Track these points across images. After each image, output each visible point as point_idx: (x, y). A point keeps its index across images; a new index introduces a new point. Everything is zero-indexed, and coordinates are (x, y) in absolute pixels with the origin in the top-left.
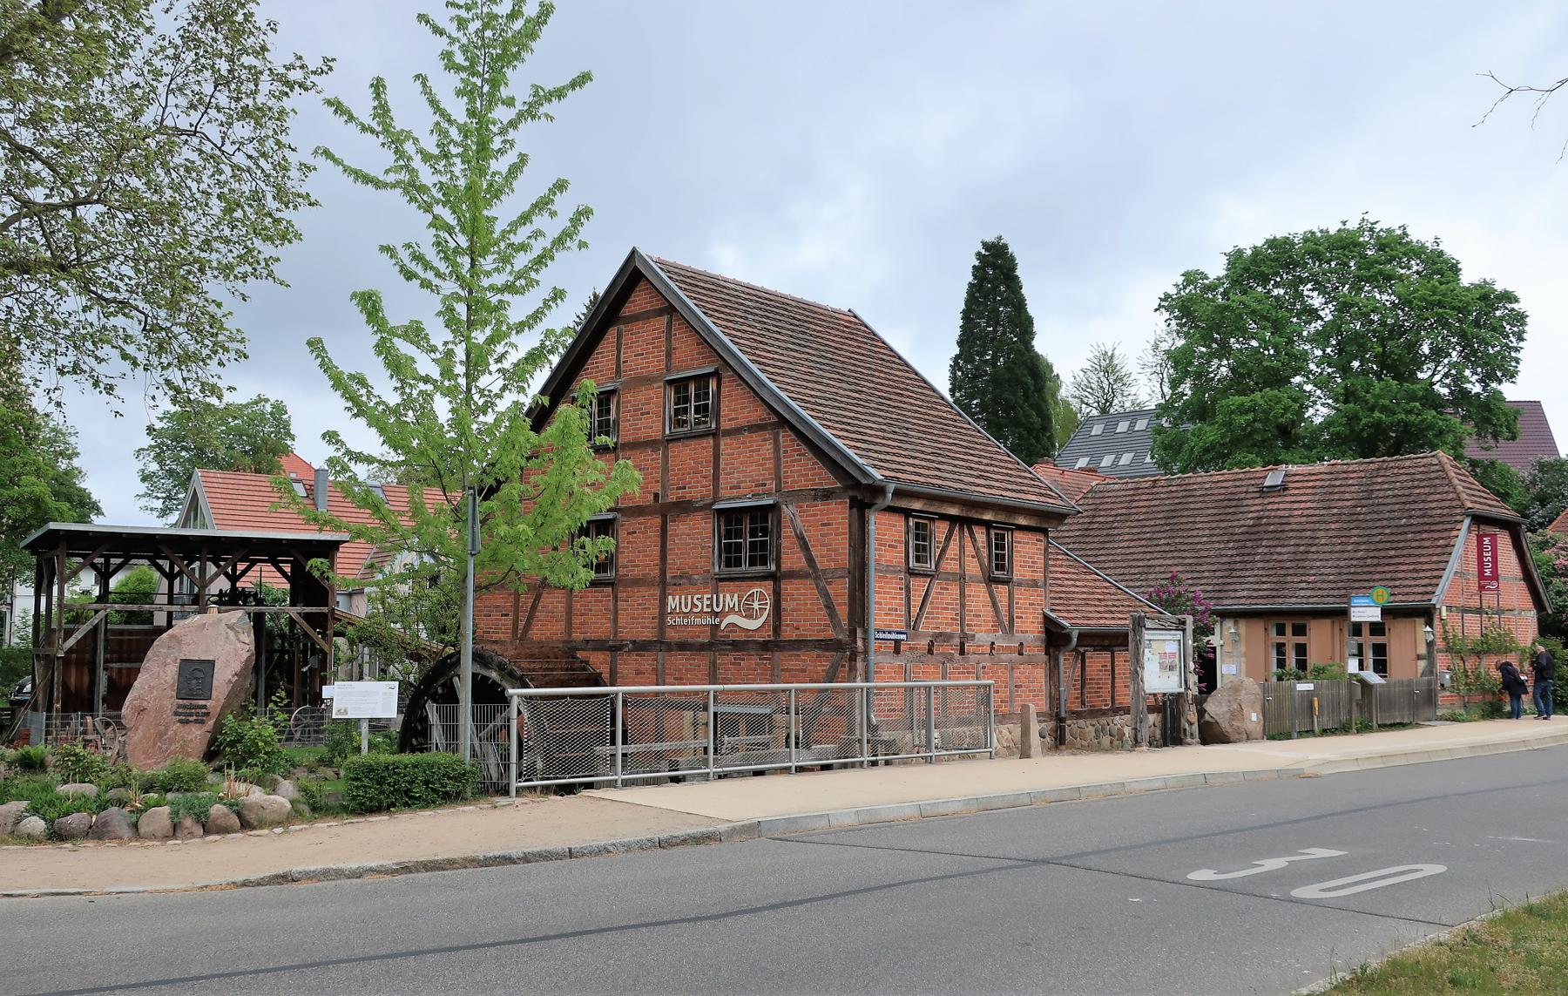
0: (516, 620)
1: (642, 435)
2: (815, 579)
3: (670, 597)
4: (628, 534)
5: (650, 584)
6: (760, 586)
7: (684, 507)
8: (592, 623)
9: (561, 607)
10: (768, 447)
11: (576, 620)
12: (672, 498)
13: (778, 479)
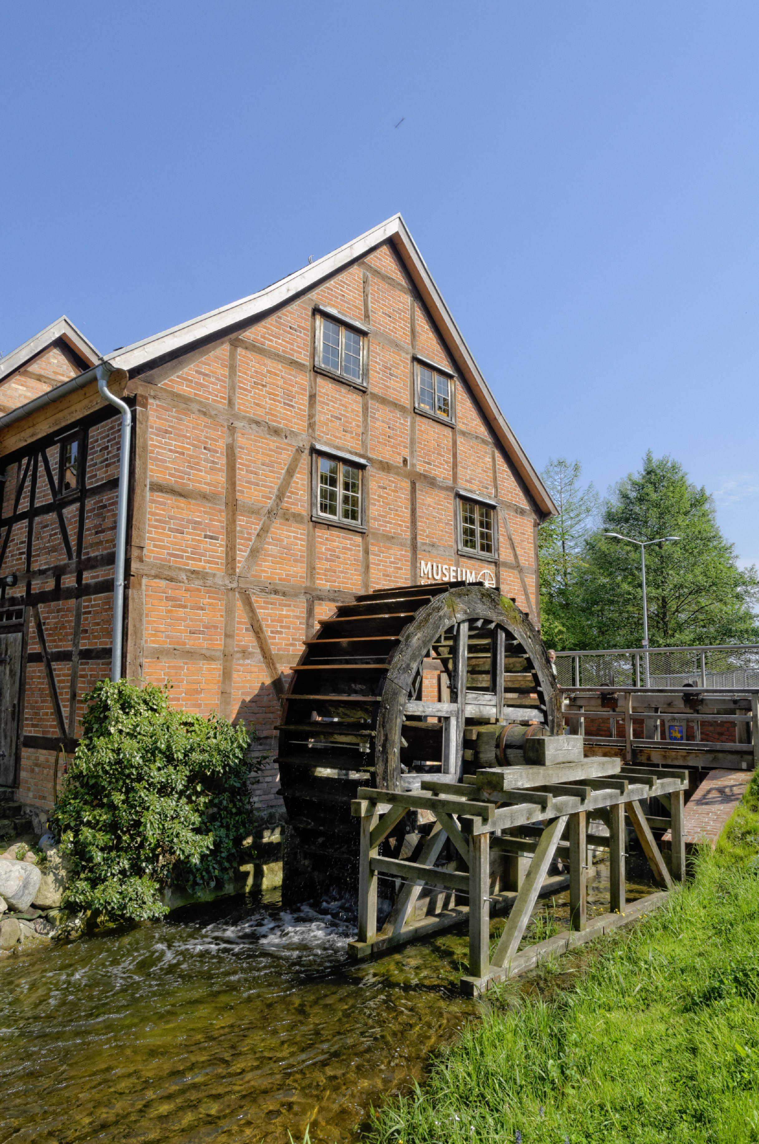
1: (392, 396)
2: (520, 572)
3: (423, 562)
4: (379, 487)
5: (402, 545)
6: (488, 568)
7: (431, 482)
8: (342, 572)
9: (300, 547)
10: (488, 459)
11: (321, 566)
12: (420, 468)
13: (496, 487)
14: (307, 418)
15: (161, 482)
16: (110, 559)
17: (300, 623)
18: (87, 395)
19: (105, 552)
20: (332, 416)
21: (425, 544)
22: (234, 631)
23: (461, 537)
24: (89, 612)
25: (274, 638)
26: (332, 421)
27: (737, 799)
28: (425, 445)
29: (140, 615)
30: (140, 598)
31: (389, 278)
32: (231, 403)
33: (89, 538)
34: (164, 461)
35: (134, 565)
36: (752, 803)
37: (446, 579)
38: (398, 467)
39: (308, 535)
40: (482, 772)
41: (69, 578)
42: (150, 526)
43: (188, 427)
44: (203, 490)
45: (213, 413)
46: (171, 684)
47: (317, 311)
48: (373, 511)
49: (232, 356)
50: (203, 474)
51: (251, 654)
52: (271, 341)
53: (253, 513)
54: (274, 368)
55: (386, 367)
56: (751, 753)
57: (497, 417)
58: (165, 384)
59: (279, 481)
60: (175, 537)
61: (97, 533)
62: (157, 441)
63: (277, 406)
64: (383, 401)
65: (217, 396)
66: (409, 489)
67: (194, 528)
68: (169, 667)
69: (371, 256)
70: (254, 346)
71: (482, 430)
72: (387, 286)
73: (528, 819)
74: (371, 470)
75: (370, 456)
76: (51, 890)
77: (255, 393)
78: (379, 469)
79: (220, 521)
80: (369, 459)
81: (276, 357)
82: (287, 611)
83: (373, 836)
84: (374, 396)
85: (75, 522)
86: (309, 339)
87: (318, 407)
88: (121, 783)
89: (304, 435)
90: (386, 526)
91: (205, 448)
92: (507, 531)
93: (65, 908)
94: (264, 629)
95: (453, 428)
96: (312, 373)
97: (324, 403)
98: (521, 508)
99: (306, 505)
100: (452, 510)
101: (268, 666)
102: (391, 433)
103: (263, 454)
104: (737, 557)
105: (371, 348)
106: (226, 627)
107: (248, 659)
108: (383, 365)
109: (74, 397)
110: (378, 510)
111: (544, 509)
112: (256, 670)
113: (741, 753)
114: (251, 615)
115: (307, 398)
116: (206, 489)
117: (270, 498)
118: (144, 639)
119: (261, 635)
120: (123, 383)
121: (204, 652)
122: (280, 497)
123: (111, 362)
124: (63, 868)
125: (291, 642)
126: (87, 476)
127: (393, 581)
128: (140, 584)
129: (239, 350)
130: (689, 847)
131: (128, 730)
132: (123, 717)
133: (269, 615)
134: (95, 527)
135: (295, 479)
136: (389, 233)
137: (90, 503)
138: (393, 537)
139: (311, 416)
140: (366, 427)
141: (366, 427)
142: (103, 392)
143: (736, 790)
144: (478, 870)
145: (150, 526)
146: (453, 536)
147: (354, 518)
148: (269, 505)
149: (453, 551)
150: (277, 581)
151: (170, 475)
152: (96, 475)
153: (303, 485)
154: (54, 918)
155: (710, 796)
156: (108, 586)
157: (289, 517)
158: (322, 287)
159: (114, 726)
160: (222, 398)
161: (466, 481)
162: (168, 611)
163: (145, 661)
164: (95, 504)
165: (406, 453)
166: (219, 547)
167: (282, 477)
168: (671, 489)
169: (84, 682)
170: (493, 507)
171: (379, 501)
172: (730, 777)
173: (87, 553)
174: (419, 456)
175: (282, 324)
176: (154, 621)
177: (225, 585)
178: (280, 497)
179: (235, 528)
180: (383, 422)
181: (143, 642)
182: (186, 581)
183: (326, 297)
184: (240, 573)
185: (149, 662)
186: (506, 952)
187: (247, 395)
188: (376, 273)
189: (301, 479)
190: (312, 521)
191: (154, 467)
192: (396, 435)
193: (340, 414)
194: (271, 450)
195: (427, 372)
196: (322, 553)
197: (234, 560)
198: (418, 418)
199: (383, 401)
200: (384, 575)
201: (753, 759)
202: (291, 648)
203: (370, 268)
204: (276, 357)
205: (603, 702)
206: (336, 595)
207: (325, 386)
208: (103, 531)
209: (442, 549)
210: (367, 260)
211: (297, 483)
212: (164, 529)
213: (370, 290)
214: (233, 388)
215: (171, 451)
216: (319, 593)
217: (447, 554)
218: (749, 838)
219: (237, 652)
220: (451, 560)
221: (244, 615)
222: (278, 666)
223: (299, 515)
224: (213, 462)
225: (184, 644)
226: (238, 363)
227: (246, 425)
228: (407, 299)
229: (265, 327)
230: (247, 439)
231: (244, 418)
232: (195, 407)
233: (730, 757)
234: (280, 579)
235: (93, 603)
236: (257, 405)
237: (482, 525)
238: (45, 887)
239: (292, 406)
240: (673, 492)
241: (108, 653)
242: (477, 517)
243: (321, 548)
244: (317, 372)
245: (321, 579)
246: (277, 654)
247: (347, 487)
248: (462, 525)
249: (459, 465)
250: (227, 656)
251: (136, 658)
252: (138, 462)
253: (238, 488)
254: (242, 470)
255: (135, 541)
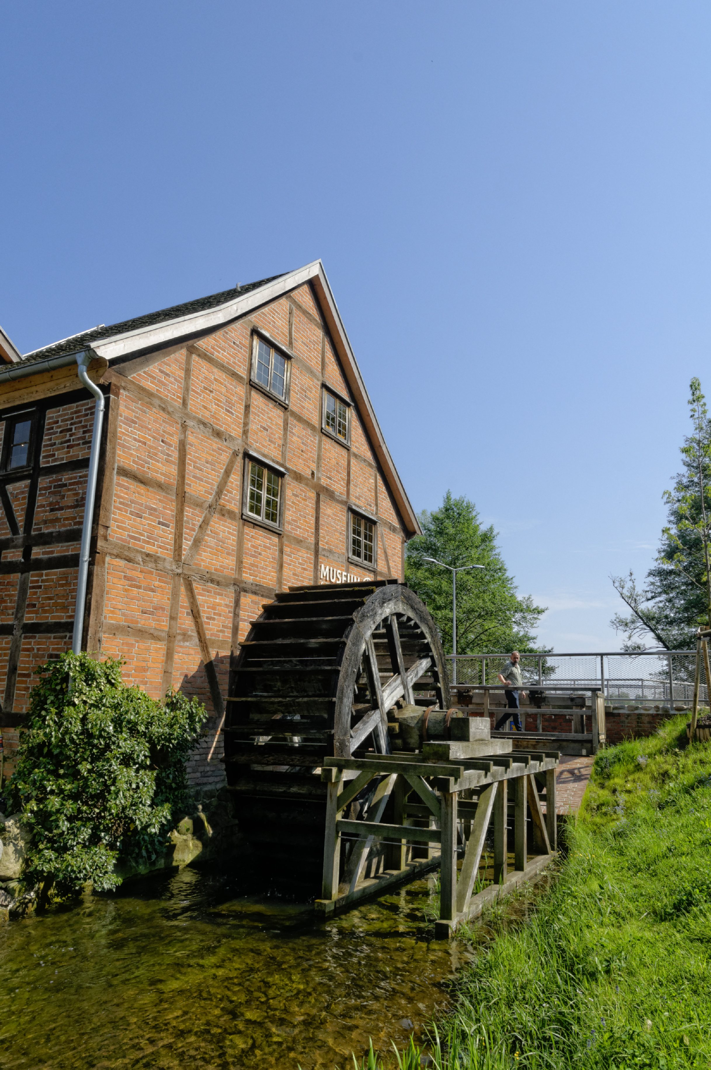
0: (179, 537)
1: (306, 415)
3: (323, 566)
4: (293, 494)
5: (308, 548)
7: (331, 494)
8: (263, 568)
9: (232, 541)
11: (247, 560)
12: (324, 482)
13: (377, 505)
14: (242, 426)
15: (126, 467)
16: (76, 535)
17: (229, 612)
18: (54, 378)
19: (63, 529)
20: (261, 426)
21: (324, 549)
22: (177, 614)
23: (351, 546)
24: (40, 587)
25: (208, 624)
26: (261, 431)
27: (586, 779)
28: (328, 462)
29: (102, 591)
30: (103, 575)
31: (309, 313)
32: (185, 403)
33: (40, 514)
34: (129, 448)
35: (100, 543)
36: (599, 781)
37: (338, 582)
38: (307, 479)
39: (239, 532)
40: (429, 745)
41: (13, 552)
42: (115, 507)
43: (150, 419)
44: (159, 479)
45: (171, 409)
46: (124, 660)
47: (255, 332)
48: (289, 515)
49: (188, 362)
50: (160, 465)
51: (190, 636)
52: (219, 352)
53: (197, 505)
54: (220, 376)
55: (303, 390)
56: (590, 741)
57: (382, 444)
58: (134, 378)
59: (219, 480)
60: (135, 520)
61: (52, 510)
62: (124, 429)
63: (220, 410)
64: (300, 419)
65: (174, 395)
66: (315, 499)
67: (150, 514)
68: (123, 644)
69: (296, 292)
70: (206, 355)
71: (368, 455)
72: (306, 319)
73: (478, 782)
74: (287, 478)
75: (288, 466)
76: (12, 861)
77: (204, 397)
78: (293, 478)
79: (172, 511)
80: (287, 469)
81: (222, 367)
82: (220, 599)
83: (340, 800)
84: (293, 414)
85: (24, 498)
86: (247, 355)
87: (251, 417)
88: (88, 753)
89: (240, 441)
90: (297, 530)
91: (163, 441)
92: (383, 545)
93: (24, 879)
94: (202, 614)
95: (348, 450)
96: (248, 386)
97: (255, 414)
98: (394, 526)
99: (238, 503)
100: (345, 522)
101: (203, 650)
102: (304, 448)
103: (207, 453)
104: (516, 588)
105: (293, 371)
106: (171, 609)
107: (187, 641)
108: (301, 388)
109: (37, 378)
110: (291, 516)
111: (410, 529)
112: (192, 652)
113: (582, 742)
114: (191, 600)
115: (243, 407)
116: (162, 479)
117: (211, 494)
118: (104, 614)
119: (198, 620)
120: (101, 372)
121: (152, 631)
122: (219, 493)
123: (96, 350)
124: (22, 839)
125: (221, 628)
126: (42, 455)
127: (301, 581)
128: (104, 562)
129: (194, 357)
130: (560, 818)
131: (92, 702)
132: (86, 689)
133: (206, 602)
134: (50, 504)
135: (230, 479)
136: (312, 275)
137: (43, 482)
138: (301, 541)
139: (246, 424)
140: (285, 440)
141: (285, 440)
142: (83, 376)
143: (583, 771)
144: (449, 824)
145: (115, 507)
146: (345, 545)
147: (274, 520)
148: (210, 500)
149: (344, 559)
150: (213, 571)
151: (134, 462)
152: (54, 455)
153: (237, 485)
154: (14, 890)
155: (563, 776)
156: (74, 561)
157: (225, 513)
158: (259, 312)
159: (78, 697)
160: (178, 397)
161: (356, 497)
162: (126, 590)
163: (104, 636)
164: (50, 482)
165: (314, 466)
166: (169, 535)
167: (221, 476)
168: (466, 525)
169: (28, 656)
170: (374, 523)
171: (292, 507)
172: (575, 761)
173: (40, 529)
174: (324, 471)
175: (228, 339)
176: (114, 599)
177: (172, 570)
178: (219, 493)
179: (183, 518)
180: (298, 437)
181: (103, 618)
182: (141, 563)
183: (262, 321)
184: (185, 560)
185: (107, 638)
186: (465, 899)
187: (197, 398)
188: (299, 307)
189: (235, 479)
190: (242, 518)
191: (121, 453)
192: (307, 450)
193: (267, 425)
194: (213, 450)
195: (332, 399)
196: (249, 549)
197: (180, 547)
198: (324, 438)
199: (300, 419)
200: (294, 574)
201: (592, 747)
202: (221, 634)
203: (294, 302)
204: (222, 367)
205: (459, 699)
206: (257, 588)
207: (257, 400)
208: (61, 509)
209: (336, 555)
210: (293, 294)
211: (232, 483)
212: (126, 512)
213: (294, 320)
214: (187, 389)
215: (135, 439)
216: (244, 585)
217: (340, 560)
218: (604, 809)
219: (179, 634)
220: (343, 566)
221: (186, 599)
222: (210, 650)
223: (233, 512)
224: (168, 455)
225: (137, 622)
226: (192, 368)
227: (196, 426)
228: (320, 333)
229: (215, 340)
230: (196, 437)
231: (195, 418)
232: (156, 402)
233: (572, 745)
234: (216, 570)
235: (44, 578)
236: (205, 407)
237: (366, 539)
238: (6, 858)
239: (232, 414)
240: (468, 529)
241: (69, 627)
242: (362, 529)
243: (247, 544)
244: (252, 385)
245: (246, 573)
246: (210, 639)
247: (269, 491)
248: (351, 535)
249: (352, 483)
250: (171, 637)
251: (96, 633)
252: (109, 447)
253: (186, 481)
254: (190, 465)
255: (102, 521)
